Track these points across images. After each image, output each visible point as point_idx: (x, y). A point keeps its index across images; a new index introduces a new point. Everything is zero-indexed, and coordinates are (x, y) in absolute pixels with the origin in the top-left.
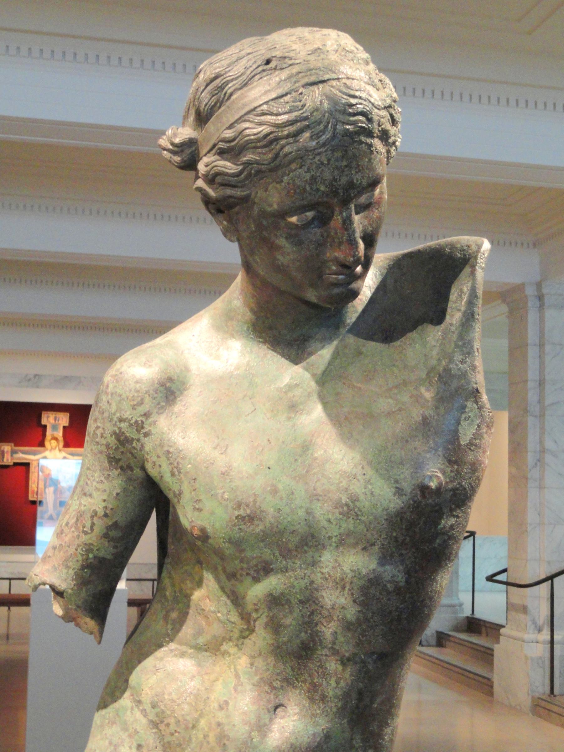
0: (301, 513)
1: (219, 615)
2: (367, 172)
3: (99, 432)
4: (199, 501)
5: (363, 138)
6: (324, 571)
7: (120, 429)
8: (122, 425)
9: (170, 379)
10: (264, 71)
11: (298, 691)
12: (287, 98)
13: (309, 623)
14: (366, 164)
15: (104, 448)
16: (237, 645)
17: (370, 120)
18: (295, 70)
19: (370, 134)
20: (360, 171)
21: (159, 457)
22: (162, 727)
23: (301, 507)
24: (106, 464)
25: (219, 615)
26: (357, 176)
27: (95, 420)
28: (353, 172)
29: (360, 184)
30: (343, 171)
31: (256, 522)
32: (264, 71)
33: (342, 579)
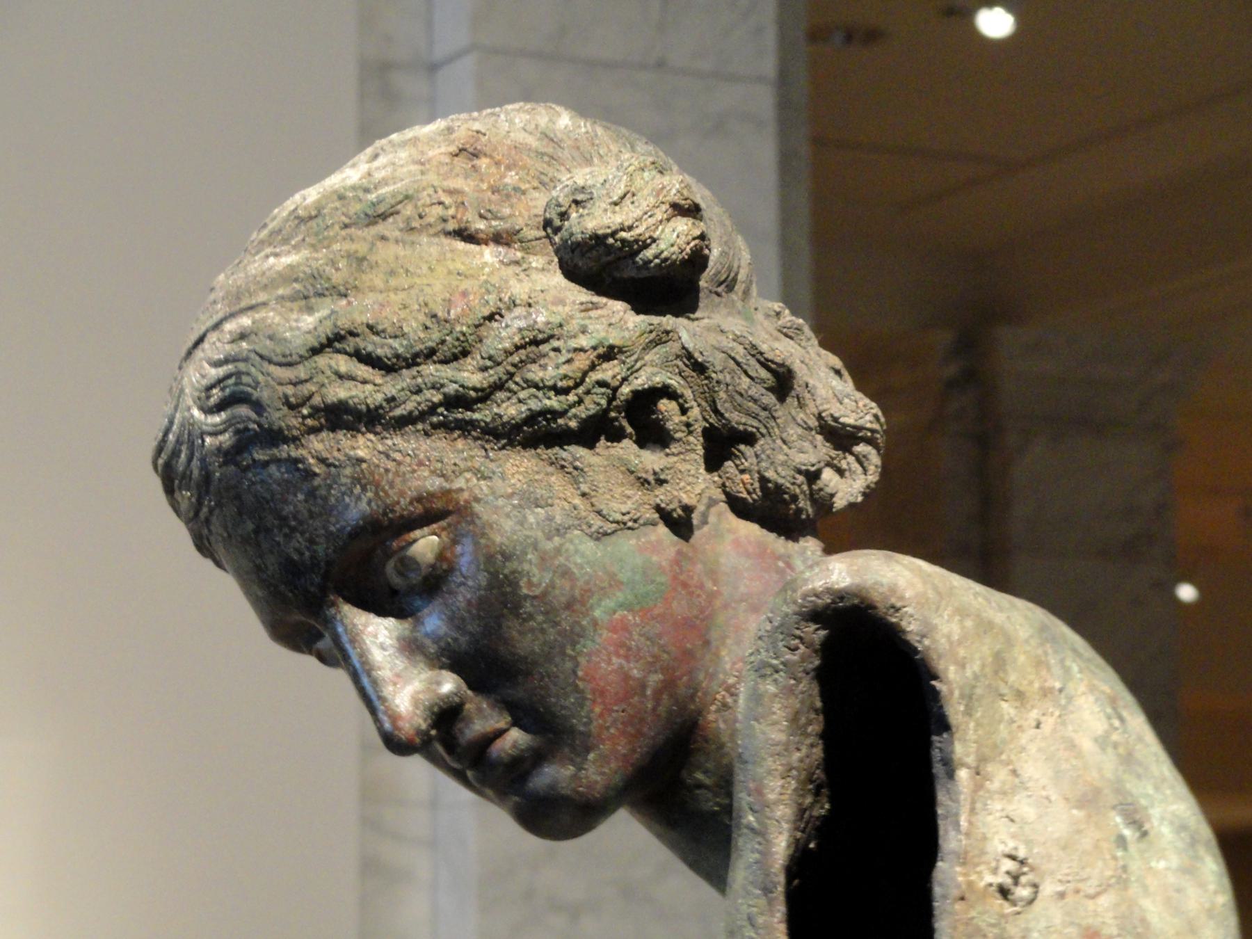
2: (317, 523)
5: (260, 455)
14: (301, 507)
17: (258, 406)
19: (275, 437)
20: (293, 530)
26: (294, 544)
28: (279, 539)
29: (312, 557)
30: (258, 545)
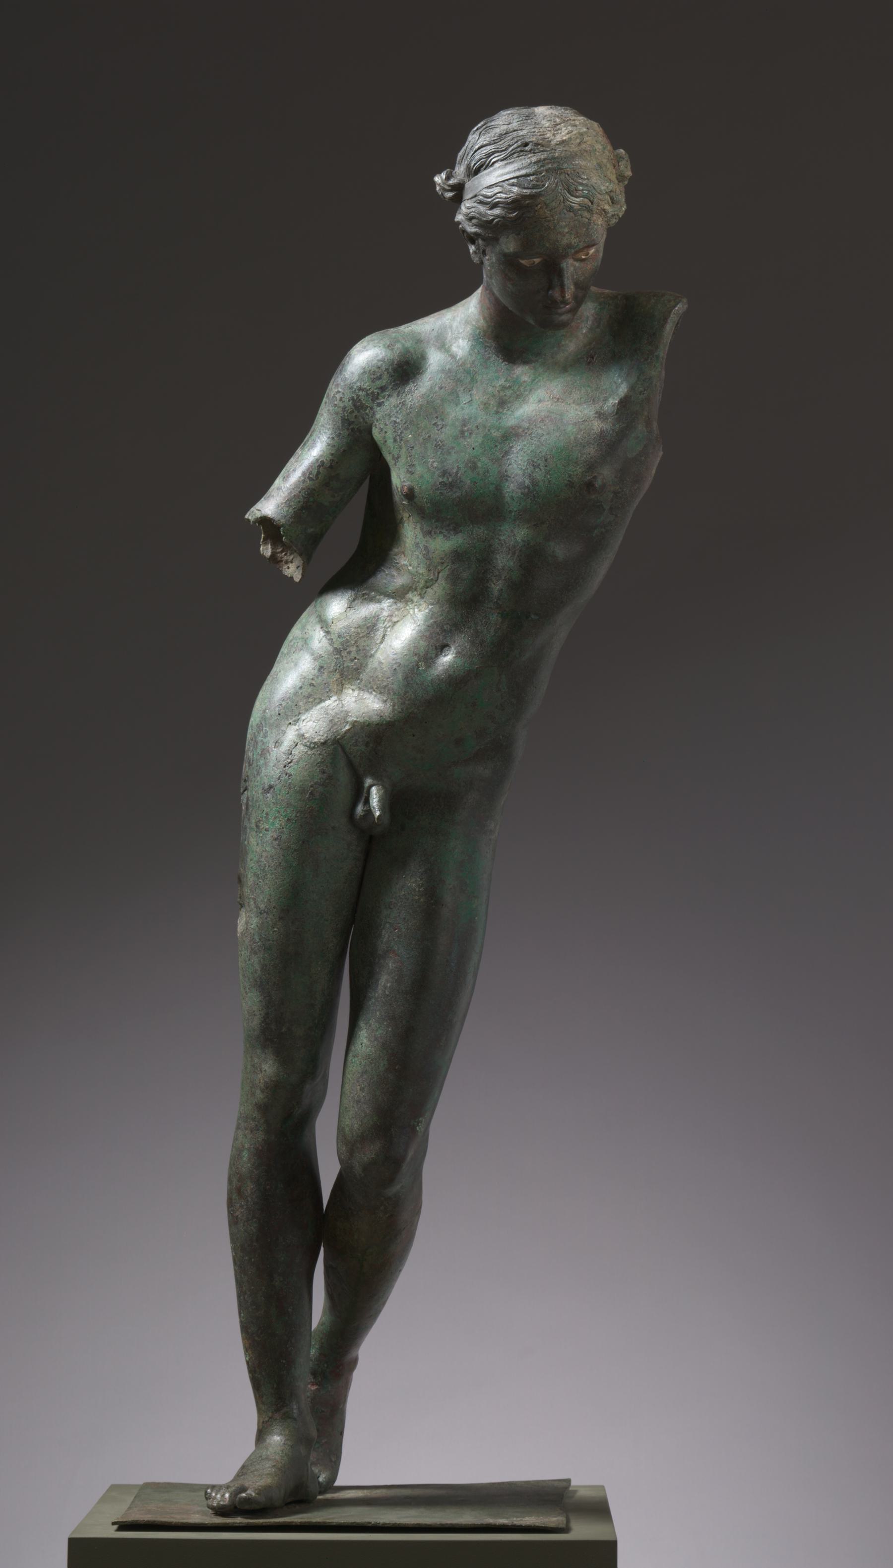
0: (492, 488)
1: (410, 568)
3: (338, 396)
4: (413, 465)
6: (502, 538)
7: (358, 396)
8: (361, 393)
9: (407, 363)
10: (521, 151)
11: (463, 636)
12: (531, 178)
13: (481, 580)
15: (340, 410)
16: (420, 594)
18: (543, 156)
21: (386, 425)
22: (344, 654)
23: (492, 484)
24: (340, 424)
25: (410, 568)
27: (337, 385)
31: (454, 490)
32: (521, 151)
33: (514, 547)
